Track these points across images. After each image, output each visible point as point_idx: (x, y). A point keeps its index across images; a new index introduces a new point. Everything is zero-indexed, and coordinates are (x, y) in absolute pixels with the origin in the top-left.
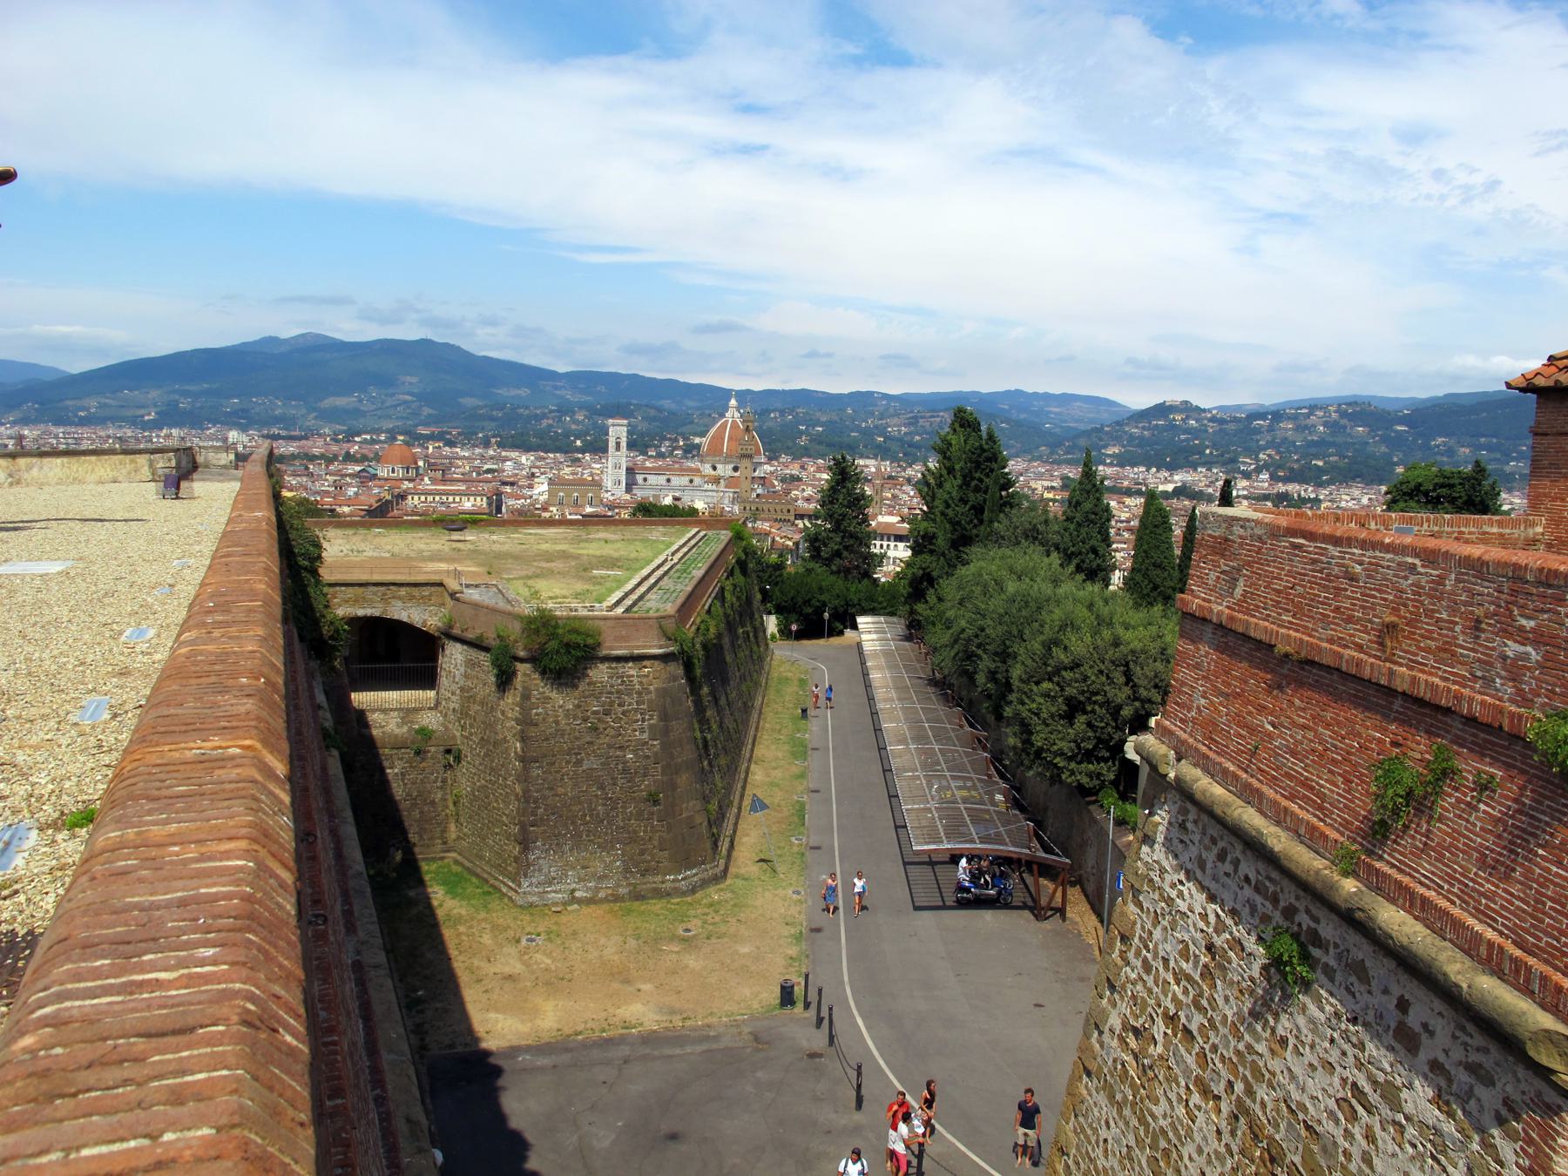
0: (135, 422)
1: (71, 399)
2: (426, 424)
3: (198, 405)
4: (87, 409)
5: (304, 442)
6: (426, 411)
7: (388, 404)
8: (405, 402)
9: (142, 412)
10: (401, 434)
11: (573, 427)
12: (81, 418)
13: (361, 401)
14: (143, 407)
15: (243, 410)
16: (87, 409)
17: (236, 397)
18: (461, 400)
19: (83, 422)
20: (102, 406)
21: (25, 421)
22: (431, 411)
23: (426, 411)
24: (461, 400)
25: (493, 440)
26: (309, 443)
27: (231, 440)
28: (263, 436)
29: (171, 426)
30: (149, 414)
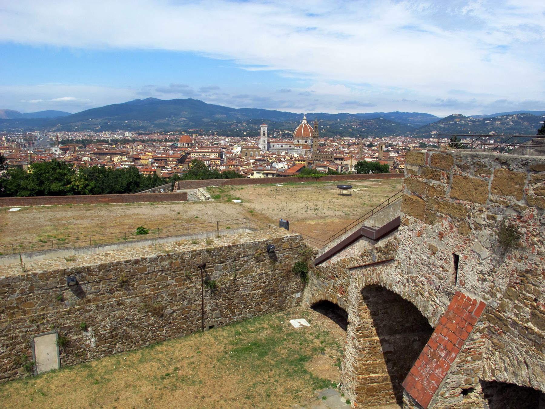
2: (191, 128)
4: (78, 126)
6: (191, 123)
10: (183, 132)
11: (242, 128)
12: (76, 129)
14: (96, 125)
16: (78, 126)
18: (203, 120)
19: (76, 130)
21: (58, 130)
22: (193, 123)
23: (191, 123)
24: (203, 120)
25: (215, 133)
26: (152, 135)
27: (126, 136)
28: (137, 133)
29: (105, 131)
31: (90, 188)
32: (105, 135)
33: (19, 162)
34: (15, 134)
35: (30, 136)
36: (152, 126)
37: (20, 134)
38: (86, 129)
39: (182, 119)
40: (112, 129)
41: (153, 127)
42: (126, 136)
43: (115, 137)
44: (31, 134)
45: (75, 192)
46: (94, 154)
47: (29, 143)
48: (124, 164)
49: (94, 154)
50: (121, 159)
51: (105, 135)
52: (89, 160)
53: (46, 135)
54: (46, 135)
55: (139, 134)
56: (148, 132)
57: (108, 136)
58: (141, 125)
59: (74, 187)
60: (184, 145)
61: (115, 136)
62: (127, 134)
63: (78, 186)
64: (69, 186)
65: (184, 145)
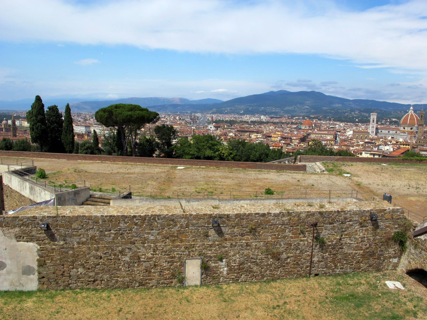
0: (239, 114)
1: (224, 108)
2: (313, 114)
4: (227, 110)
5: (280, 119)
6: (313, 111)
7: (302, 109)
8: (307, 108)
10: (306, 117)
11: (355, 115)
15: (265, 110)
16: (227, 110)
17: (263, 107)
18: (323, 108)
19: (226, 113)
20: (231, 109)
21: (213, 113)
22: (314, 111)
24: (323, 108)
25: (332, 119)
26: (282, 119)
27: (261, 118)
28: (270, 117)
29: (247, 114)
31: (232, 156)
32: (247, 118)
33: (186, 134)
34: (185, 115)
35: (194, 117)
36: (282, 112)
37: (188, 115)
38: (233, 113)
40: (252, 113)
41: (283, 113)
42: (261, 118)
43: (254, 119)
44: (195, 115)
45: (222, 158)
46: (238, 131)
47: (193, 122)
48: (259, 140)
49: (238, 131)
50: (257, 136)
51: (247, 118)
52: (234, 136)
53: (205, 116)
54: (205, 116)
55: (272, 118)
56: (278, 116)
57: (248, 118)
59: (221, 154)
60: (306, 127)
61: (254, 118)
62: (262, 117)
63: (224, 154)
64: (217, 153)
65: (306, 127)
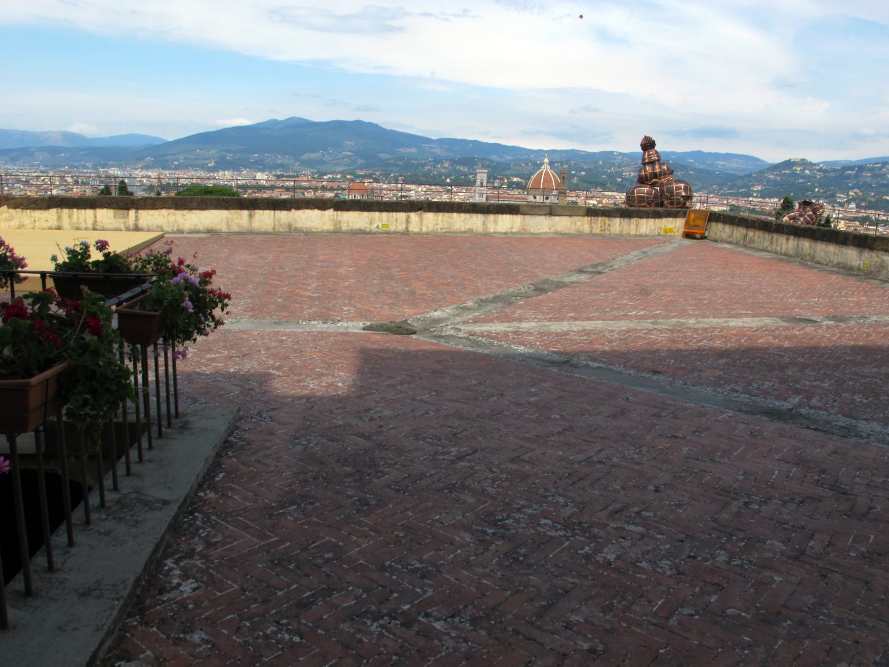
0: (203, 167)
2: (361, 169)
3: (236, 158)
4: (178, 160)
6: (360, 161)
7: (338, 157)
8: (348, 156)
9: (206, 162)
11: (443, 171)
13: (324, 155)
15: (260, 160)
16: (178, 160)
17: (256, 153)
18: (380, 155)
20: (186, 159)
21: (147, 167)
23: (360, 161)
24: (380, 155)
25: (400, 178)
28: (274, 175)
29: (224, 170)
30: (211, 163)
36: (298, 163)
39: (346, 153)
41: (300, 165)
44: (106, 172)
55: (278, 177)
56: (290, 174)
58: (279, 162)
62: (259, 176)
